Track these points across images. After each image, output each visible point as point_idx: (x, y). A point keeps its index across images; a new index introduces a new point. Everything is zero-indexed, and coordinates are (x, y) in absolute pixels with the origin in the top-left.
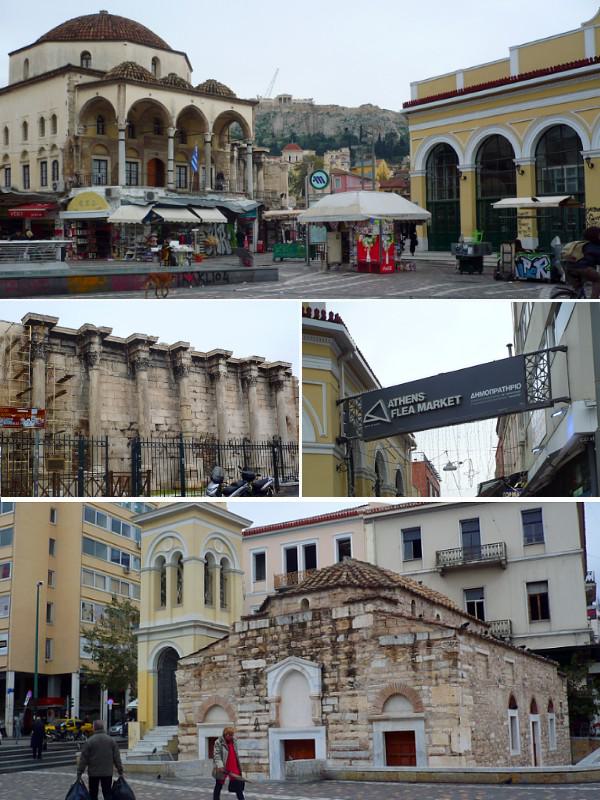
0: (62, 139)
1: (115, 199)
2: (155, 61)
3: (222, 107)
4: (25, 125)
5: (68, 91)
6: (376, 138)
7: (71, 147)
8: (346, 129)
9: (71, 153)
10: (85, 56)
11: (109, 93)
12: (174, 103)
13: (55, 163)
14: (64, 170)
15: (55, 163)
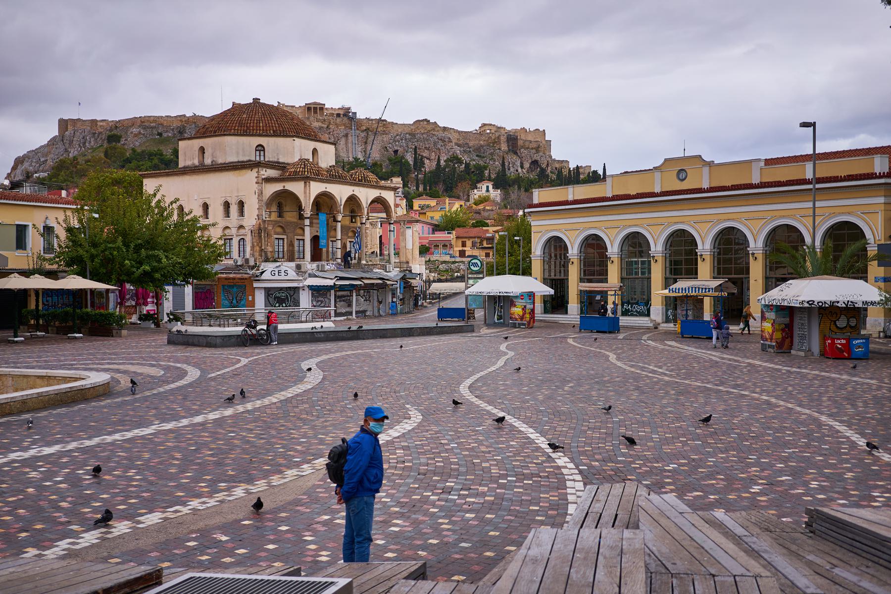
0: (251, 220)
1: (305, 272)
2: (315, 151)
3: (373, 193)
4: (206, 207)
6: (434, 164)
7: (260, 229)
8: (396, 152)
9: (260, 237)
10: (260, 148)
11: (296, 187)
12: (341, 192)
14: (253, 247)
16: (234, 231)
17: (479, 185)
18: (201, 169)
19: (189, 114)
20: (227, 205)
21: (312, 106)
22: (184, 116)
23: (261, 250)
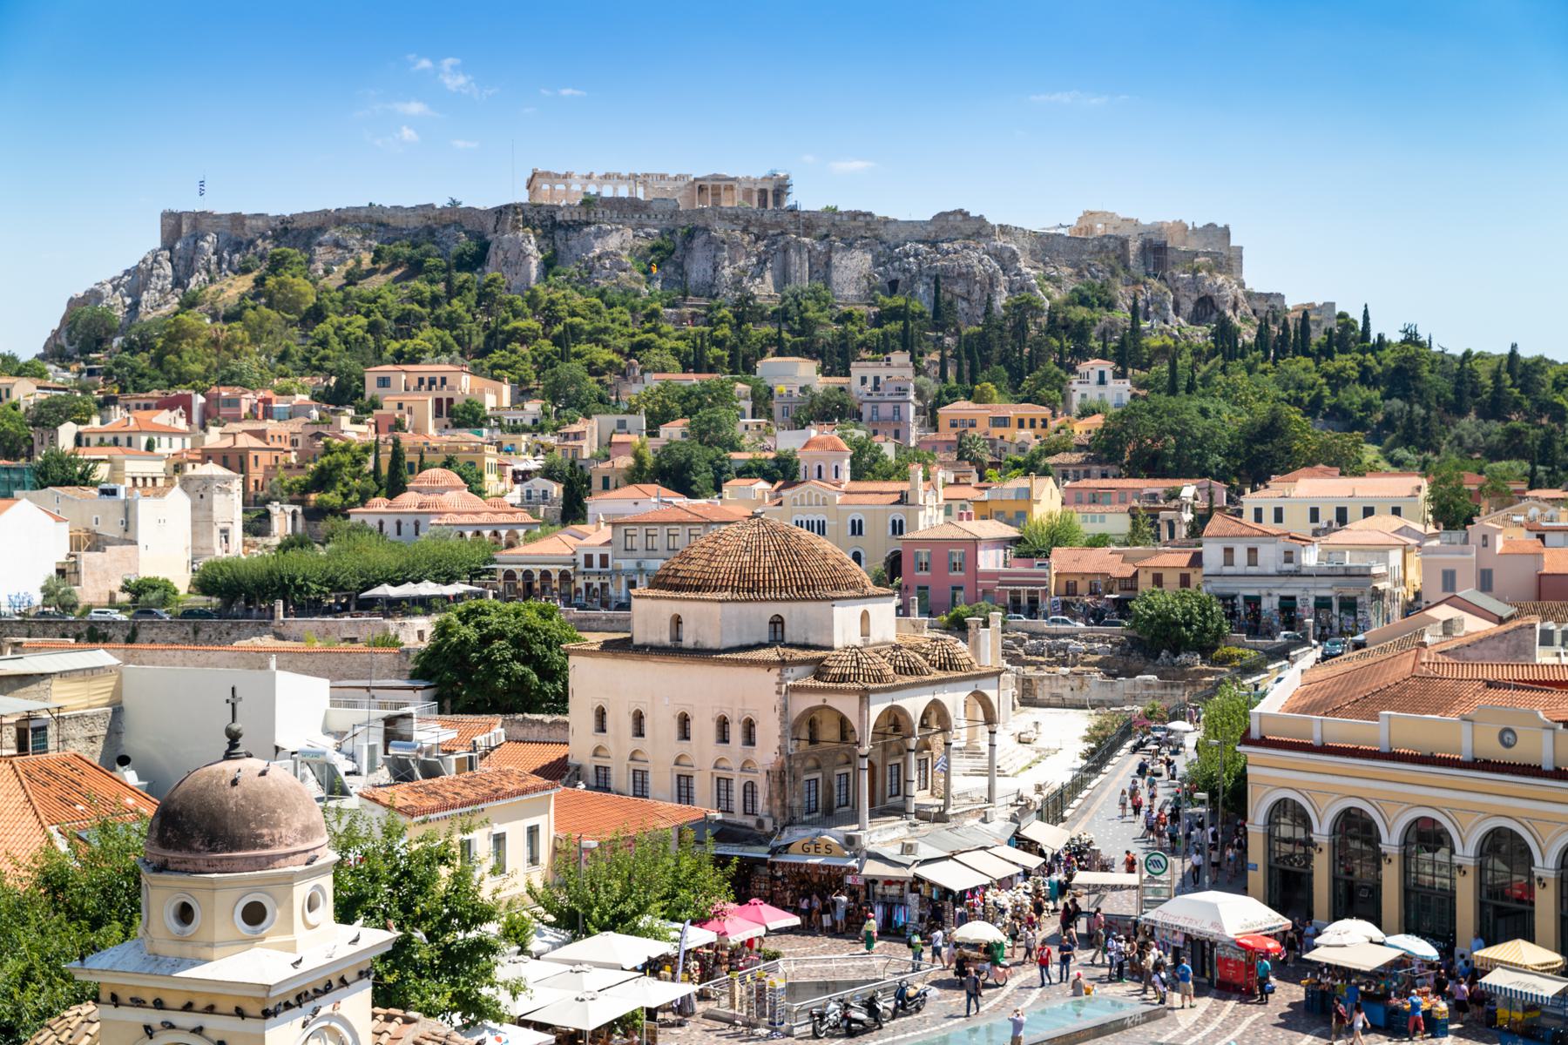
0: (767, 752)
4: (684, 721)
5: (779, 693)
7: (782, 771)
9: (782, 782)
10: (777, 622)
12: (914, 704)
13: (750, 789)
14: (770, 799)
15: (750, 789)
16: (735, 765)
17: (1083, 367)
18: (674, 650)
19: (441, 202)
20: (723, 724)
21: (709, 184)
22: (432, 206)
23: (783, 805)
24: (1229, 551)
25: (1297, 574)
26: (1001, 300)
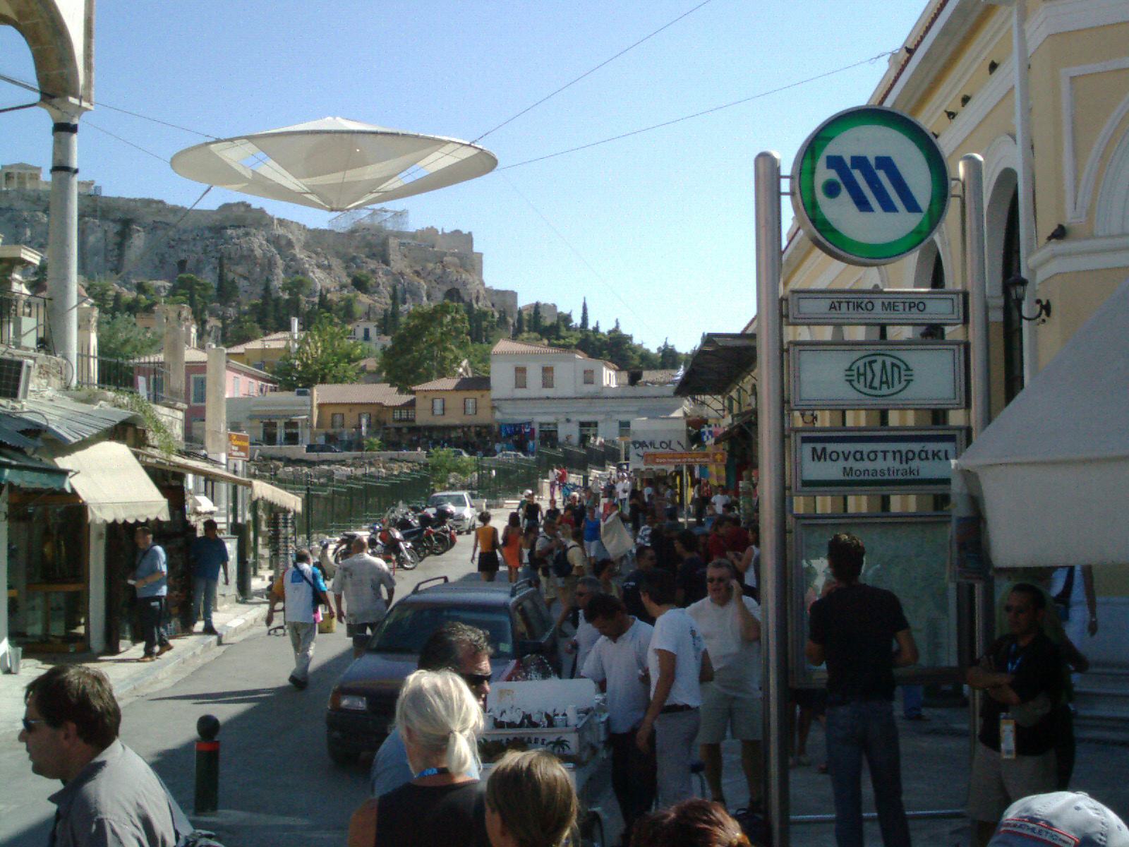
21: (15, 171)
24: (521, 371)
25: (595, 397)
26: (279, 278)
